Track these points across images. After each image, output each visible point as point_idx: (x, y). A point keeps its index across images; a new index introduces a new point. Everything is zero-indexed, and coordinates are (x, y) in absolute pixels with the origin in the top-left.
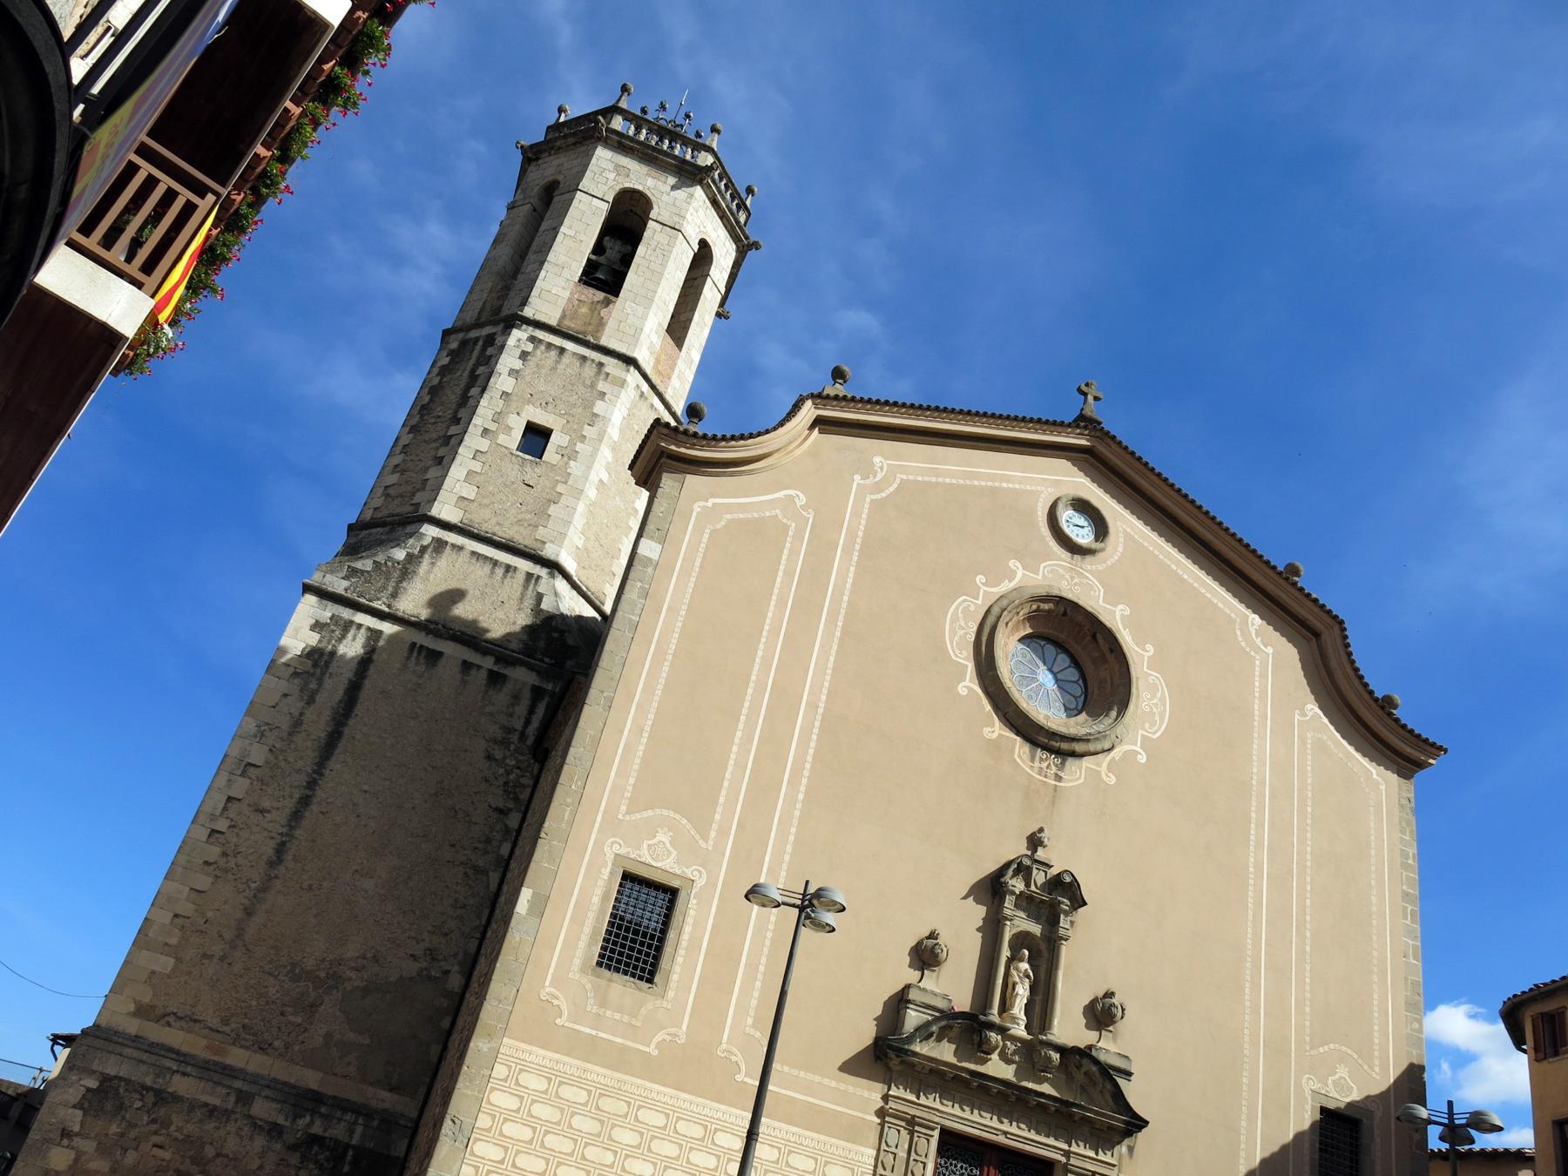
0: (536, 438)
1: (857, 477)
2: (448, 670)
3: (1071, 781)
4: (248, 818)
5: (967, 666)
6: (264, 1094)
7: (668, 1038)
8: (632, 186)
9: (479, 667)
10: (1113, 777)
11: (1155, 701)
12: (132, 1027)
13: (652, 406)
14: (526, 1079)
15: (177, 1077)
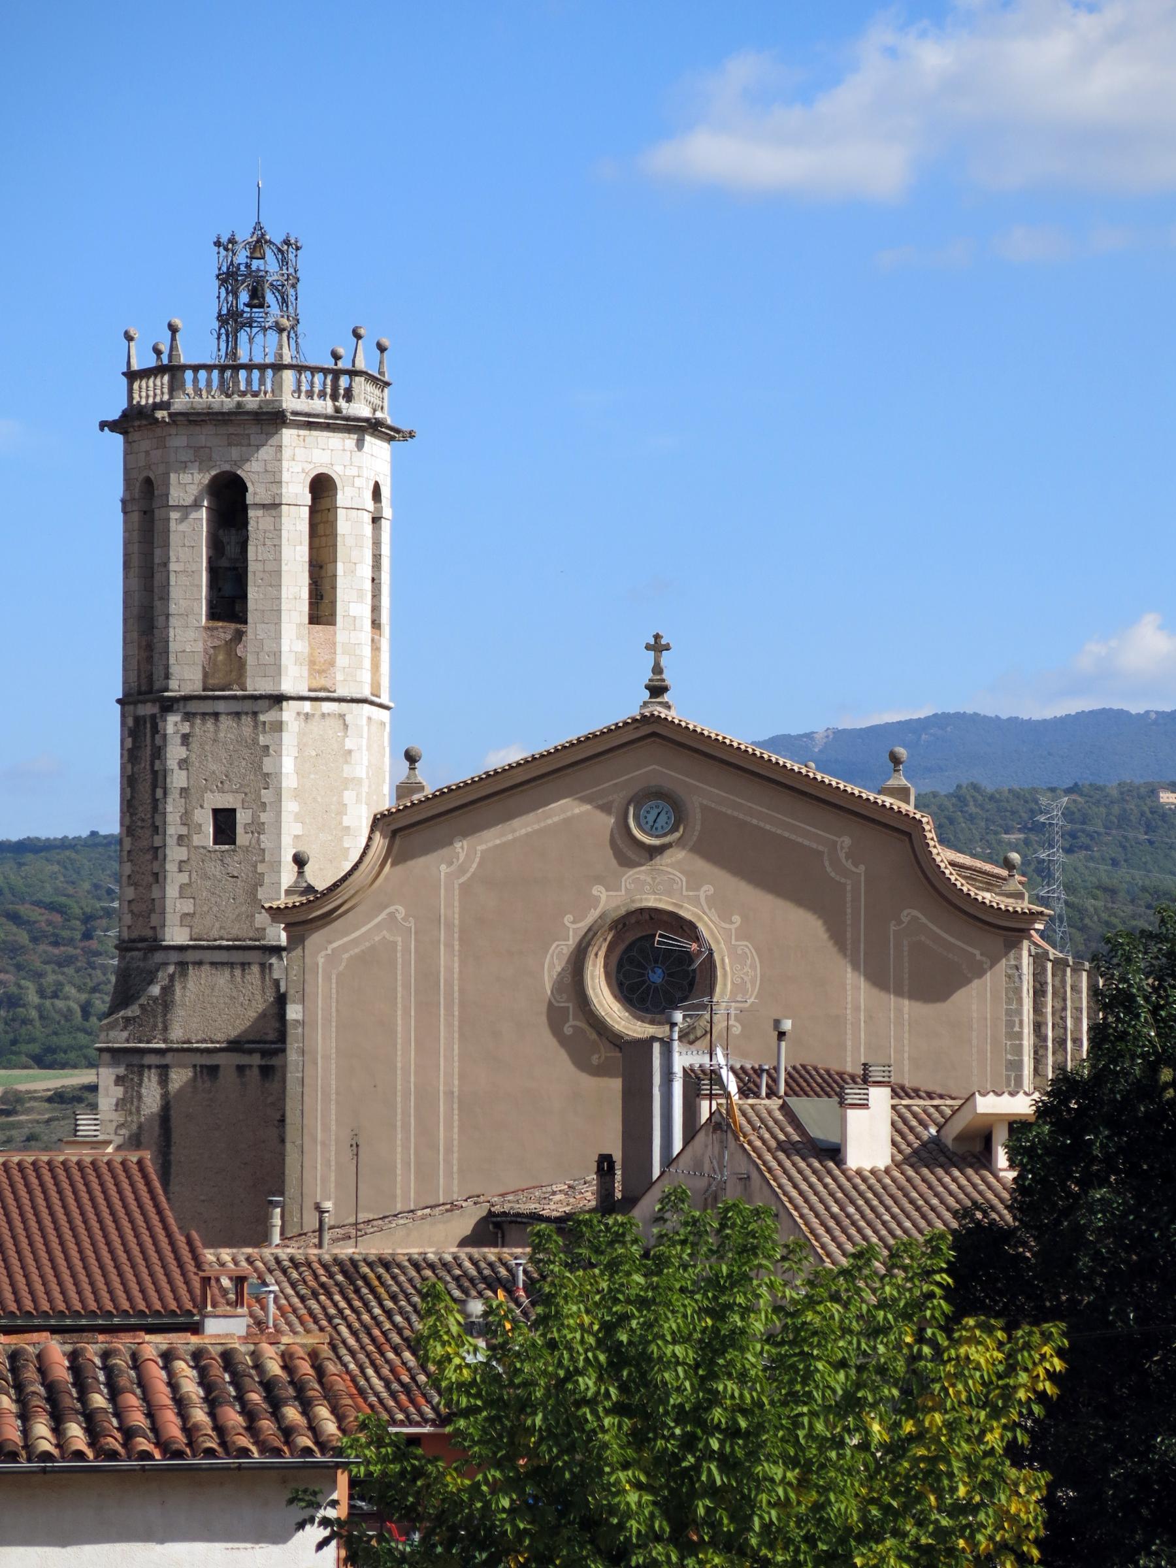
0: (225, 823)
1: (443, 867)
2: (228, 1077)
9: (251, 1066)
13: (323, 715)
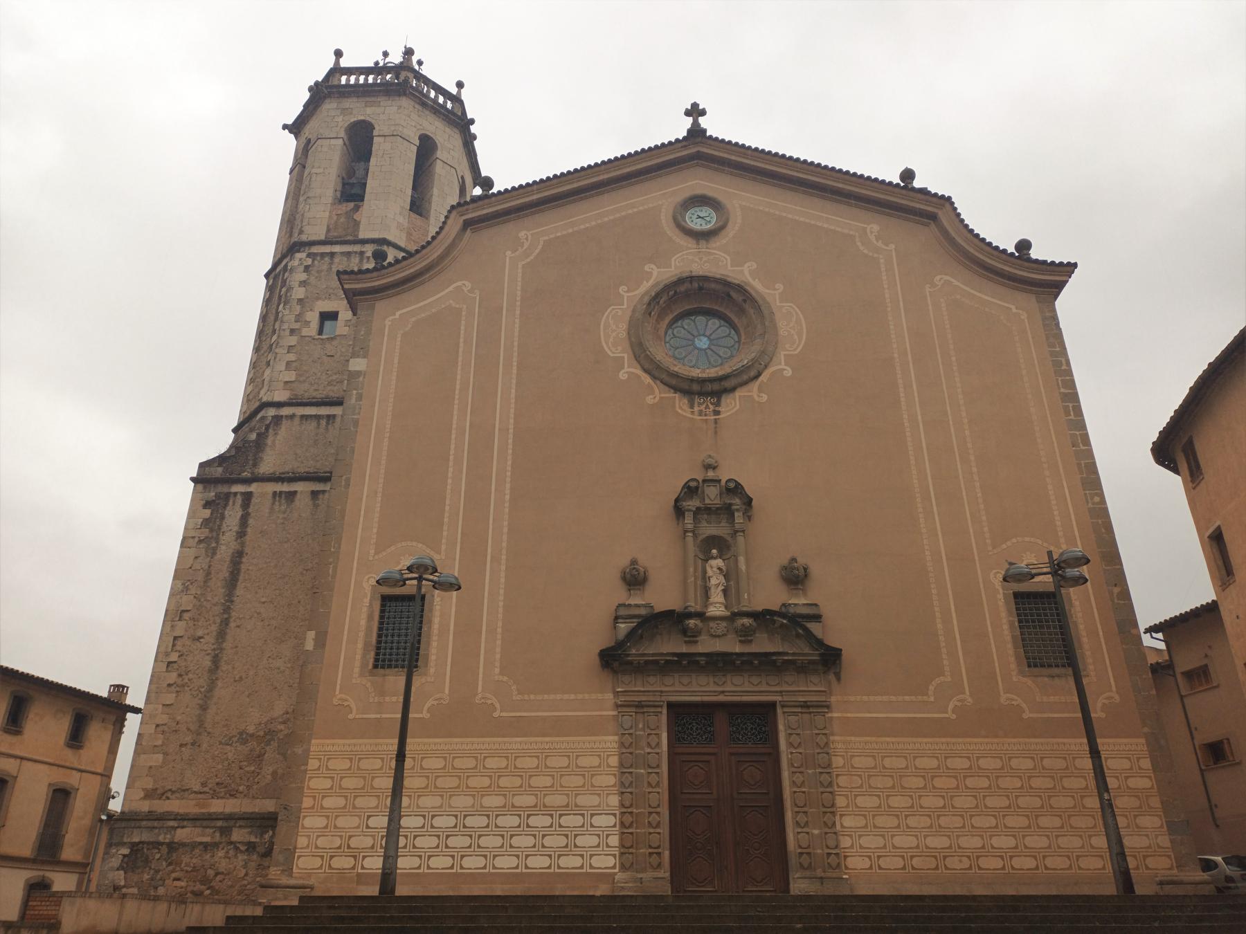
1: (508, 253)
2: (303, 502)
3: (728, 411)
4: (190, 646)
5: (623, 357)
6: (238, 825)
7: (435, 703)
8: (356, 119)
10: (763, 395)
11: (791, 325)
12: (145, 806)
14: (331, 764)
15: (179, 831)
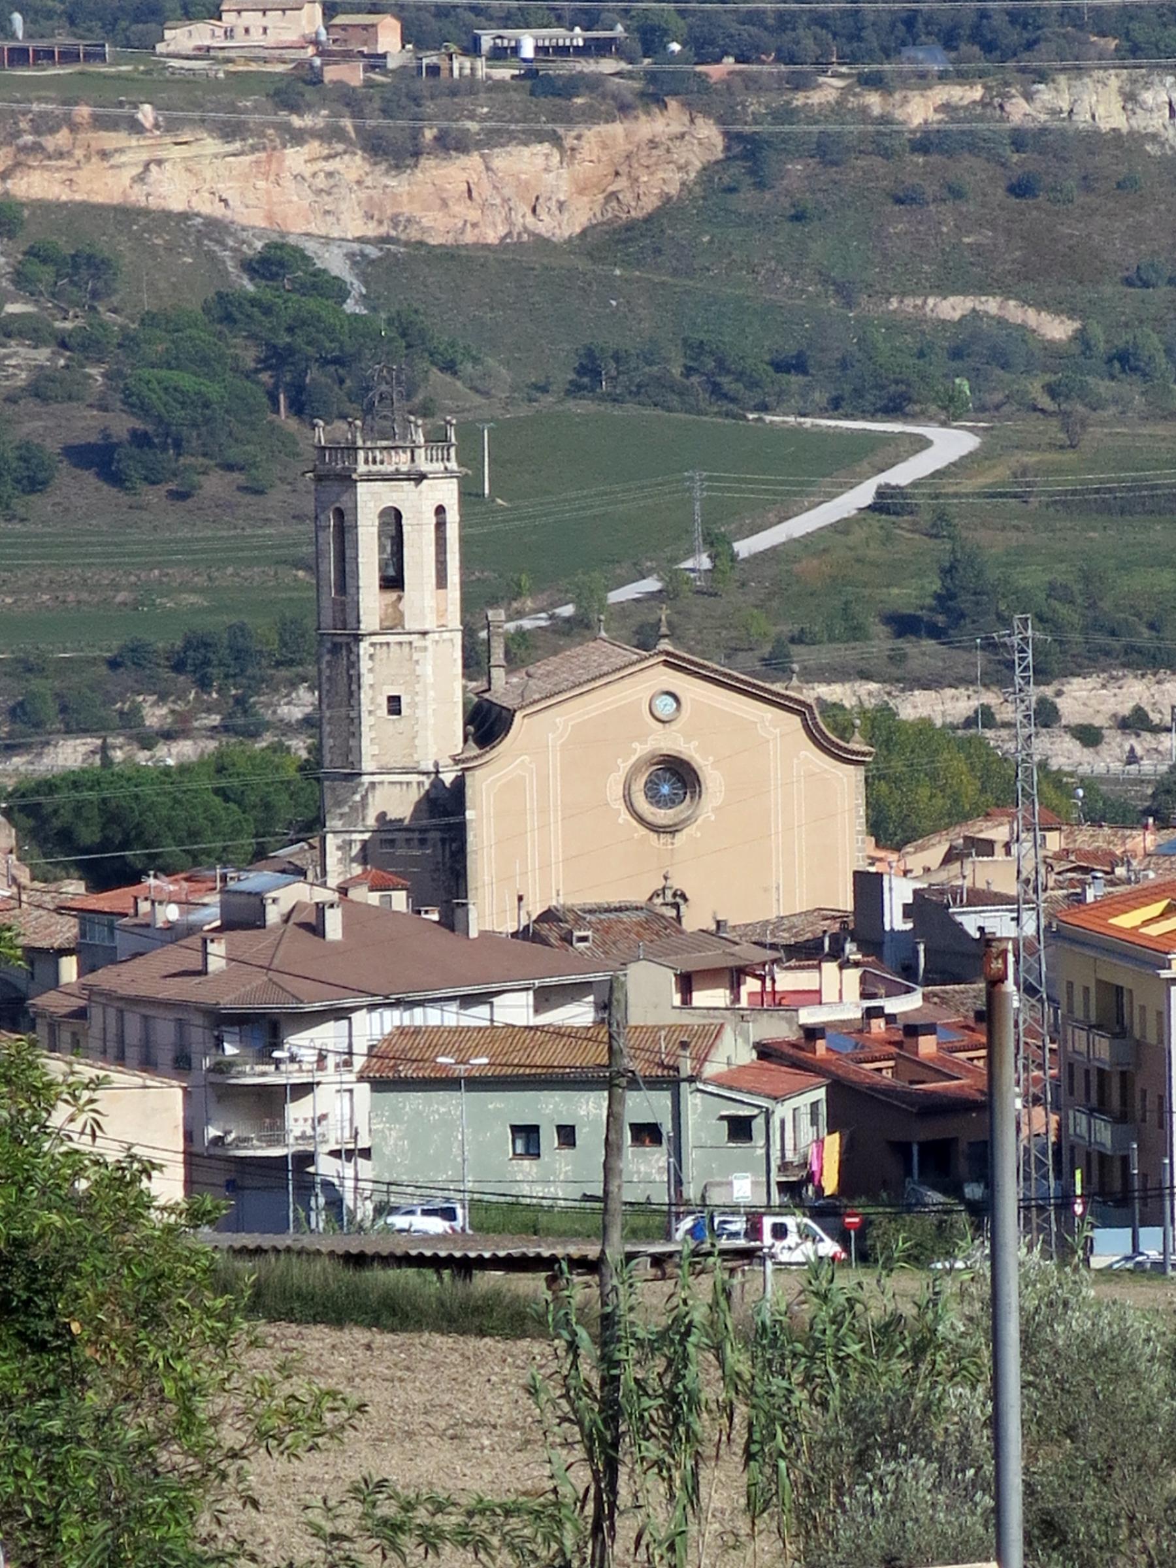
0: (395, 706)
